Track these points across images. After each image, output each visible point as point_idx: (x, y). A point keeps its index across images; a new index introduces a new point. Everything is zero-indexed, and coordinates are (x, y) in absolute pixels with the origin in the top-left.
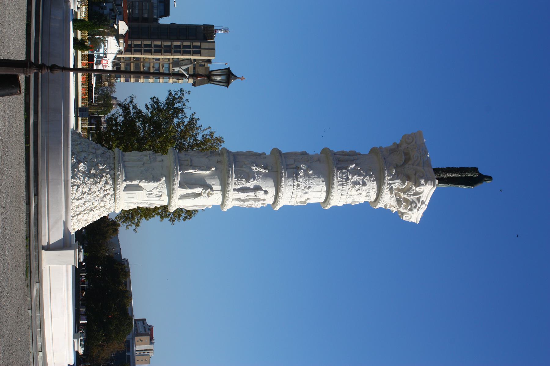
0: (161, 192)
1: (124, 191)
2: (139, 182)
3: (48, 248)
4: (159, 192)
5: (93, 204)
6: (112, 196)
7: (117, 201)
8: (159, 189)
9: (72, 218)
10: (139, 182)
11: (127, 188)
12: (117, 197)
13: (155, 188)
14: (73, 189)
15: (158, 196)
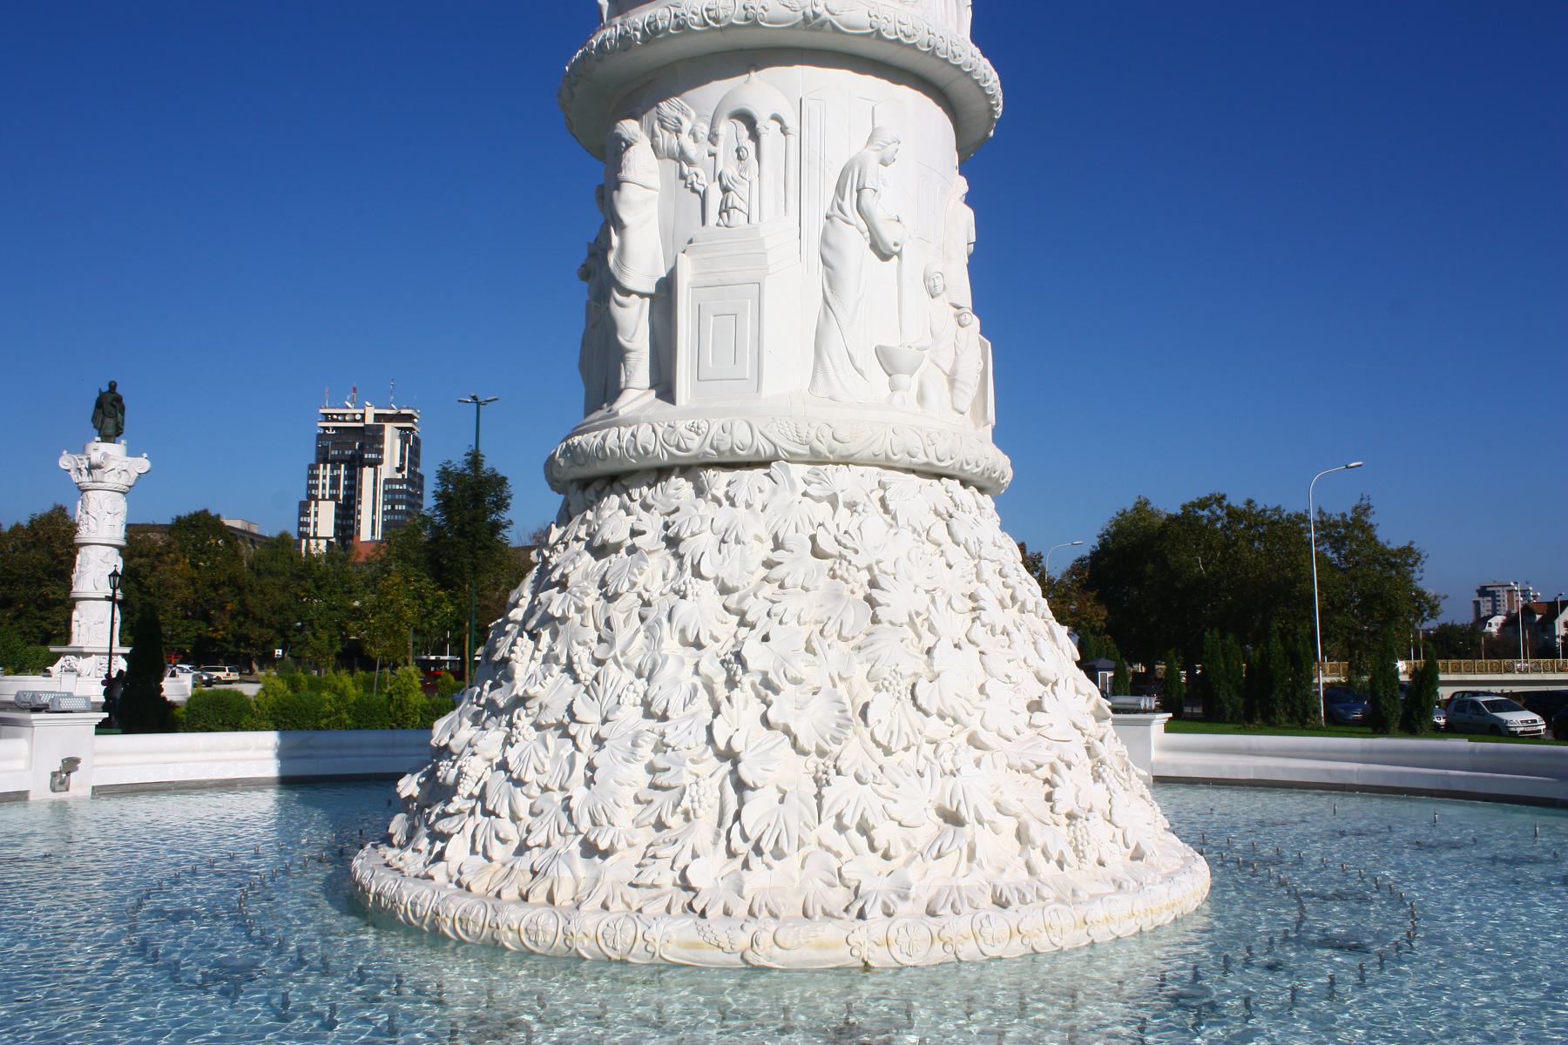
0: (713, 125)
1: (672, 401)
2: (628, 293)
4: (713, 138)
5: (691, 638)
6: (700, 491)
7: (742, 439)
8: (686, 140)
9: (745, 839)
10: (628, 293)
11: (664, 386)
12: (695, 445)
13: (682, 177)
14: (504, 811)
15: (751, 146)
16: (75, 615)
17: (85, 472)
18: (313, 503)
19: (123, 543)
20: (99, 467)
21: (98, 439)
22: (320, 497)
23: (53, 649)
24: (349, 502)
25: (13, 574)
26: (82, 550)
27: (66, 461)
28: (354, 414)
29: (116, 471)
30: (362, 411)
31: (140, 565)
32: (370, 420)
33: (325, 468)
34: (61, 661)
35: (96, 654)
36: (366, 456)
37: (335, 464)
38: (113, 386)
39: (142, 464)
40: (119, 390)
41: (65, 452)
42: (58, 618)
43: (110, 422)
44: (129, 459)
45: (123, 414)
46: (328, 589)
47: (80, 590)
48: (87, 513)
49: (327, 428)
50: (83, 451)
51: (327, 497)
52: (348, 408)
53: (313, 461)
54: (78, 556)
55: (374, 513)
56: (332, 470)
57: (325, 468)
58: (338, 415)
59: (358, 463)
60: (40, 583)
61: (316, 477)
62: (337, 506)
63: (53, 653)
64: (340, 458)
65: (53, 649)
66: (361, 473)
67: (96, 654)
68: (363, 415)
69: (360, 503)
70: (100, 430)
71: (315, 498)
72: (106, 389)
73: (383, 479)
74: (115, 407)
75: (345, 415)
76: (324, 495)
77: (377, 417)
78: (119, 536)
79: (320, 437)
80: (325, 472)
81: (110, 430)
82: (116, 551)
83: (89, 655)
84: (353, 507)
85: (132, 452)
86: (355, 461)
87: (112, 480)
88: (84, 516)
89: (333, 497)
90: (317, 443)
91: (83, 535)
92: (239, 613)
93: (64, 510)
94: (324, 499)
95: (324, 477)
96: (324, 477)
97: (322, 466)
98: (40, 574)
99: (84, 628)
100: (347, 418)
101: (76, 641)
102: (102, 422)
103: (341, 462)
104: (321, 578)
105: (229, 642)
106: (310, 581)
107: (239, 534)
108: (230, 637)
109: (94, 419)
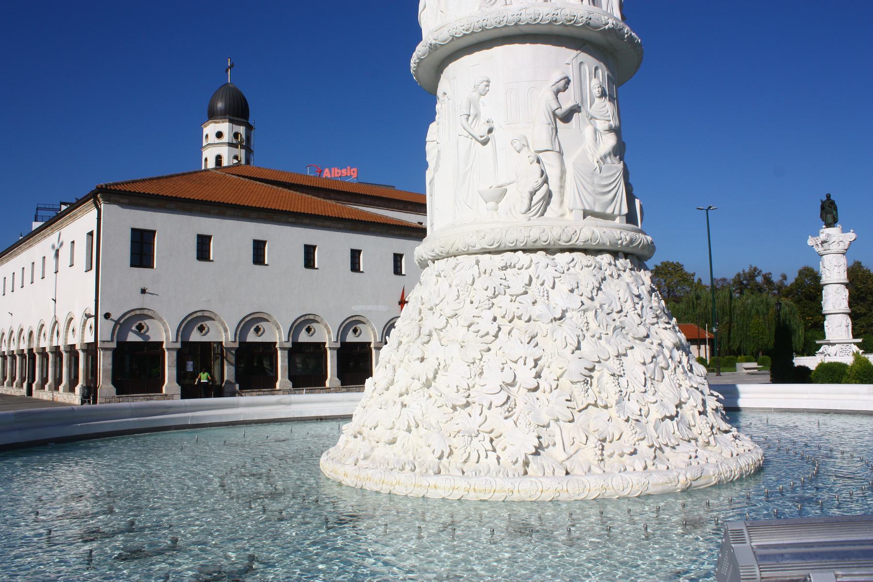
16: (826, 323)
17: (820, 245)
21: (824, 226)
23: (817, 342)
26: (825, 288)
27: (811, 242)
29: (836, 242)
35: (838, 343)
38: (828, 196)
39: (851, 236)
40: (832, 198)
41: (810, 236)
43: (829, 216)
44: (843, 234)
47: (826, 309)
63: (819, 344)
65: (817, 342)
67: (838, 343)
72: (824, 199)
78: (843, 277)
81: (830, 221)
82: (843, 286)
85: (844, 231)
87: (834, 248)
91: (824, 280)
93: (860, 263)
99: (830, 329)
109: (821, 216)
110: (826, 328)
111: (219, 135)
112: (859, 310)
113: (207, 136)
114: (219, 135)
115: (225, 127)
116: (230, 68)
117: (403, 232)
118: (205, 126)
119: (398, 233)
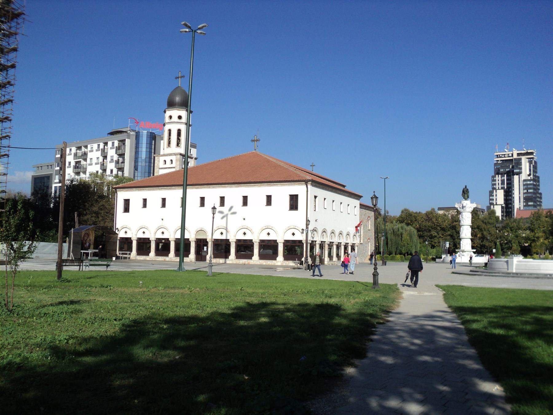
3: (508, 269)
16: (461, 242)
18: (495, 191)
19: (471, 225)
20: (465, 207)
21: (464, 200)
22: (497, 188)
24: (509, 189)
25: (423, 229)
28: (509, 154)
30: (512, 153)
31: (456, 225)
32: (515, 156)
33: (498, 177)
34: (459, 253)
35: (467, 251)
36: (515, 171)
37: (502, 174)
38: (466, 187)
41: (456, 203)
42: (436, 241)
44: (471, 204)
45: (469, 193)
46: (514, 231)
48: (463, 218)
49: (498, 161)
50: (461, 202)
51: (500, 188)
52: (506, 152)
53: (494, 175)
54: (461, 228)
55: (520, 194)
56: (501, 177)
57: (498, 177)
58: (502, 155)
59: (511, 174)
60: (430, 231)
61: (495, 180)
62: (504, 192)
64: (504, 172)
66: (513, 178)
67: (467, 251)
68: (512, 154)
69: (514, 190)
70: (464, 198)
71: (495, 189)
73: (522, 180)
74: (467, 192)
75: (505, 155)
76: (499, 188)
77: (519, 154)
79: (495, 164)
80: (498, 178)
81: (466, 197)
83: (466, 251)
84: (511, 192)
85: (471, 203)
86: (510, 173)
88: (462, 219)
89: (502, 188)
90: (495, 167)
91: (462, 223)
92: (482, 238)
94: (499, 189)
95: (498, 180)
96: (498, 180)
97: (497, 176)
98: (430, 228)
100: (506, 156)
101: (462, 249)
102: (464, 195)
103: (505, 174)
104: (512, 227)
105: (478, 247)
106: (509, 228)
107: (478, 210)
108: (479, 246)
109: (462, 195)
110: (461, 245)
111: (180, 117)
112: (434, 234)
113: (171, 117)
114: (180, 117)
115: (183, 113)
116: (181, 77)
117: (357, 197)
118: (169, 110)
119: (356, 197)
